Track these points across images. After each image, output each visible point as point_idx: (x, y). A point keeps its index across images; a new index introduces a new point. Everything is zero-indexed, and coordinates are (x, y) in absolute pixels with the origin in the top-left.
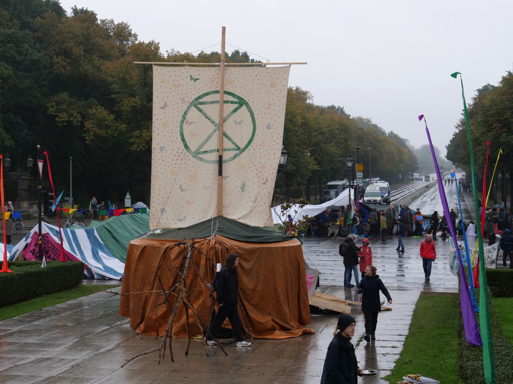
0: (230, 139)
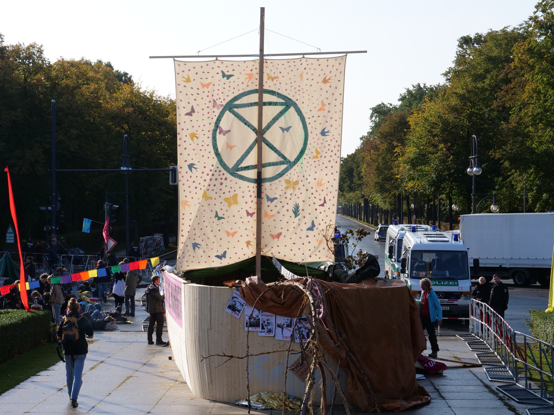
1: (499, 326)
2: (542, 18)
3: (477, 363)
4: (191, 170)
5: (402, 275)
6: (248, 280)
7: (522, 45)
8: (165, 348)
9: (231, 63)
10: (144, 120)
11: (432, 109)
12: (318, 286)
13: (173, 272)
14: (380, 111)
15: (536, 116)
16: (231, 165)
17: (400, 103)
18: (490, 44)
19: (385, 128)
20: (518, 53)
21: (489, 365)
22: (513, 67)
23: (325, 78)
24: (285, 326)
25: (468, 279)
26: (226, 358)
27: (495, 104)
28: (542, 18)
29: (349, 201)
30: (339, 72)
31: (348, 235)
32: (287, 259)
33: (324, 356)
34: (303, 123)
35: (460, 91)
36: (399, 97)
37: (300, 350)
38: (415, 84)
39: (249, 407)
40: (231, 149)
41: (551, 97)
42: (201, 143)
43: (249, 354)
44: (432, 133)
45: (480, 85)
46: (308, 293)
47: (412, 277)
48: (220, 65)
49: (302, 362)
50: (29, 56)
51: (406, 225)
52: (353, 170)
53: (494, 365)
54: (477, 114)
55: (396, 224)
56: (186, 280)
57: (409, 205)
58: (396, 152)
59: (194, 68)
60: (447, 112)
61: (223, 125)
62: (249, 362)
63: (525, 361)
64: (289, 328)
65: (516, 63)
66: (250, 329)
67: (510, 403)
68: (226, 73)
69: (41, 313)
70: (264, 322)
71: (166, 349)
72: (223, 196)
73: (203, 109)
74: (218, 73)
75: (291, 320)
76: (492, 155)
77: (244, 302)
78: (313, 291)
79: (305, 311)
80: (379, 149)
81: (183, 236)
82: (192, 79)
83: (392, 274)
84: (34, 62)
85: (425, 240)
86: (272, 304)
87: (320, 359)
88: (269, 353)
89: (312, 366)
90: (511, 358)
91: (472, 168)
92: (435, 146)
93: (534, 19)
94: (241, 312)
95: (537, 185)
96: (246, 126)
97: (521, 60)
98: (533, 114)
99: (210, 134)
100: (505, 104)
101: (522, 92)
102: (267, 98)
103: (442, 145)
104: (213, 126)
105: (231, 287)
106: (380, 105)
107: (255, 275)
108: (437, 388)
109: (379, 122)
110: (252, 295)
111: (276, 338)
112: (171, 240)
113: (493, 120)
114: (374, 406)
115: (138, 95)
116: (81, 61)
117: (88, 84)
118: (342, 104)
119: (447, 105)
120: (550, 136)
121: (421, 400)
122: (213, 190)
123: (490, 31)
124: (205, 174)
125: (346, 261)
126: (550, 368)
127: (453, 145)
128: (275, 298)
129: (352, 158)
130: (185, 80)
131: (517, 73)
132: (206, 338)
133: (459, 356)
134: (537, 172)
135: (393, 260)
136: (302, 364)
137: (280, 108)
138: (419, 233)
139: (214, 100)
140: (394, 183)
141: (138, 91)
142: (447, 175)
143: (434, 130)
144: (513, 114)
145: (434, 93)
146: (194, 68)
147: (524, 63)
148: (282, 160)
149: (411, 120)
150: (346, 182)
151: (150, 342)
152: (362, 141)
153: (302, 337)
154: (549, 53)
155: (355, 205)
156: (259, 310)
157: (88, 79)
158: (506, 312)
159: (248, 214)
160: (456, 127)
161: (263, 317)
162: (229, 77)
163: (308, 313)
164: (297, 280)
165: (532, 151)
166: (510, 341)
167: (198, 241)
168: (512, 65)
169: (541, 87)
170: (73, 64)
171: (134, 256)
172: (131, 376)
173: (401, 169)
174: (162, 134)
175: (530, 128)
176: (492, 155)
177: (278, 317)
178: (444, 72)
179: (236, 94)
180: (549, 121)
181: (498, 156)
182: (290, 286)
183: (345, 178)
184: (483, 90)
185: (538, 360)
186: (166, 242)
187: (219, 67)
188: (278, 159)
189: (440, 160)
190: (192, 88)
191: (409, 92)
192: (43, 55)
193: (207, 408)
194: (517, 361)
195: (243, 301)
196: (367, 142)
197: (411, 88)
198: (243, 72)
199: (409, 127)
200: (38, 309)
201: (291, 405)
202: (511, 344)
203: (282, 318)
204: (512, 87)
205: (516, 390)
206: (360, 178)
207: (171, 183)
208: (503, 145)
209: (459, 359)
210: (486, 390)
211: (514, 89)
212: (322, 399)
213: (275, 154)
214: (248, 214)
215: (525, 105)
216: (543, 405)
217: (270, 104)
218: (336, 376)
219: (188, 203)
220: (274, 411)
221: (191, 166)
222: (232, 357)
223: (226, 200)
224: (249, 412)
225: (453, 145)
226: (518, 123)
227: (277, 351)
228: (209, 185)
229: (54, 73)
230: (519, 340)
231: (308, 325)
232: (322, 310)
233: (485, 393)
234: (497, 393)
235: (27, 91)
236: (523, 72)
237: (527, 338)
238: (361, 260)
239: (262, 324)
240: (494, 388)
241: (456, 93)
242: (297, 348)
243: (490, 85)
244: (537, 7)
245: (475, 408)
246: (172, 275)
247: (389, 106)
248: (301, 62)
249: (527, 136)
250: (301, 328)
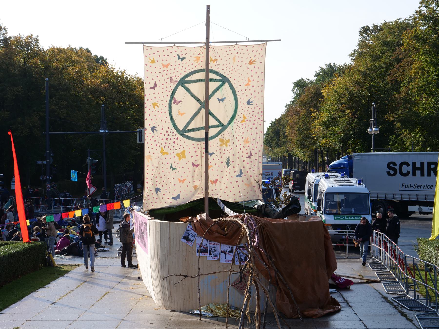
1: (394, 252)
2: (425, 12)
3: (377, 280)
4: (153, 132)
5: (318, 212)
6: (198, 217)
7: (410, 33)
8: (135, 270)
9: (185, 48)
10: (117, 93)
11: (340, 83)
12: (253, 221)
13: (140, 211)
14: (300, 85)
15: (421, 88)
16: (181, 128)
17: (316, 78)
18: (386, 31)
19: (304, 98)
20: (407, 38)
21: (386, 281)
22: (403, 50)
23: (251, 60)
24: (227, 252)
25: (369, 214)
26: (182, 278)
27: (389, 79)
28: (425, 12)
29: (277, 154)
30: (261, 56)
31: (276, 181)
32: (230, 200)
33: (258, 275)
34: (234, 96)
35: (363, 69)
36: (315, 74)
37: (239, 271)
38: (328, 63)
39: (200, 315)
41: (432, 73)
42: (160, 111)
43: (200, 274)
44: (340, 101)
45: (377, 64)
46: (245, 226)
47: (326, 213)
48: (176, 49)
49: (241, 280)
50: (28, 45)
51: (321, 173)
52: (280, 131)
53: (390, 281)
54: (375, 86)
55: (313, 172)
56: (151, 217)
57: (323, 157)
58: (313, 116)
59: (158, 52)
60: (352, 85)
61: (177, 96)
62: (200, 280)
63: (414, 277)
64: (230, 254)
65: (405, 47)
66: (201, 254)
67: (402, 310)
68: (181, 56)
69: (39, 243)
70: (211, 249)
71: (135, 271)
72: (176, 152)
73: (163, 84)
74: (175, 56)
75: (232, 248)
76: (387, 118)
77: (196, 233)
78: (249, 225)
79: (243, 241)
80: (299, 114)
81: (147, 183)
82: (156, 61)
83: (311, 211)
84: (31, 50)
85: (336, 185)
86: (217, 235)
87: (255, 278)
88: (215, 273)
89: (249, 283)
90: (403, 275)
91: (371, 128)
92: (343, 112)
93: (419, 12)
94: (193, 241)
95: (422, 141)
96: (192, 98)
97: (409, 44)
98: (419, 86)
99: (167, 104)
100: (397, 79)
101: (410, 69)
102: (212, 76)
103: (348, 111)
104: (169, 98)
105: (185, 222)
106: (300, 80)
107: (204, 213)
108: (346, 299)
109: (299, 93)
110: (202, 228)
111: (221, 262)
112: (139, 186)
113: (388, 90)
114: (297, 314)
115: (111, 73)
116: (68, 48)
117: (73, 66)
118: (263, 80)
119: (352, 80)
120: (432, 103)
121: (334, 308)
122: (168, 147)
123: (384, 22)
124: (163, 134)
125: (274, 201)
126: (433, 283)
127: (356, 111)
128: (219, 230)
129: (279, 121)
130: (151, 61)
131: (406, 55)
132: (167, 262)
133: (363, 275)
134: (422, 131)
135: (311, 200)
136: (241, 281)
137: (219, 83)
138: (331, 179)
139: (171, 77)
140: (311, 141)
141: (112, 71)
142: (353, 134)
143: (342, 99)
144: (403, 86)
145: (342, 70)
146: (158, 52)
147: (411, 47)
149: (324, 92)
150: (274, 140)
151: (123, 265)
152: (286, 108)
153: (241, 261)
154: (431, 39)
155: (281, 158)
156: (207, 240)
157: (73, 62)
158: (399, 240)
160: (359, 97)
161: (210, 245)
162: (182, 59)
163: (245, 242)
164: (237, 217)
165: (418, 115)
166: (402, 263)
167: (159, 186)
168: (402, 48)
169: (425, 65)
170: (61, 50)
171: (109, 198)
172: (109, 292)
173: (317, 129)
174: (131, 104)
175: (417, 97)
176: (387, 118)
177: (222, 245)
178: (350, 53)
179: (187, 72)
180: (431, 92)
181: (392, 119)
182: (231, 221)
183: (274, 137)
184: (380, 68)
185: (424, 277)
186: (135, 188)
187: (175, 51)
188: (216, 123)
189: (346, 122)
190: (156, 68)
191: (323, 70)
192: (38, 44)
193: (168, 316)
194: (407, 278)
195: (195, 233)
196: (291, 110)
197: (324, 67)
198: (193, 56)
199: (322, 97)
200: (36, 240)
201: (233, 313)
202: (403, 264)
203: (225, 246)
204: (402, 65)
205: (407, 300)
206: (285, 137)
207: (138, 142)
208: (396, 110)
209: (363, 276)
210: (384, 300)
211: (404, 67)
212: (257, 308)
213: (213, 119)
215: (412, 79)
216: (428, 312)
217: (211, 80)
218: (267, 290)
219: (151, 157)
220: (220, 318)
221: (153, 129)
222: (186, 276)
223: (177, 155)
224: (200, 319)
225: (356, 111)
226: (407, 93)
227: (221, 272)
228: (166, 143)
229: (47, 58)
230: (409, 262)
231: (245, 251)
232: (256, 239)
233: (383, 303)
234: (393, 303)
235: (26, 72)
236: (410, 54)
237: (415, 260)
238: (286, 201)
239: (210, 251)
240: (390, 299)
241: (359, 71)
242: (237, 269)
243: (385, 63)
244: (421, 3)
245: (376, 315)
246: (140, 213)
247: (307, 80)
248: (234, 48)
249: (414, 103)
250: (240, 253)
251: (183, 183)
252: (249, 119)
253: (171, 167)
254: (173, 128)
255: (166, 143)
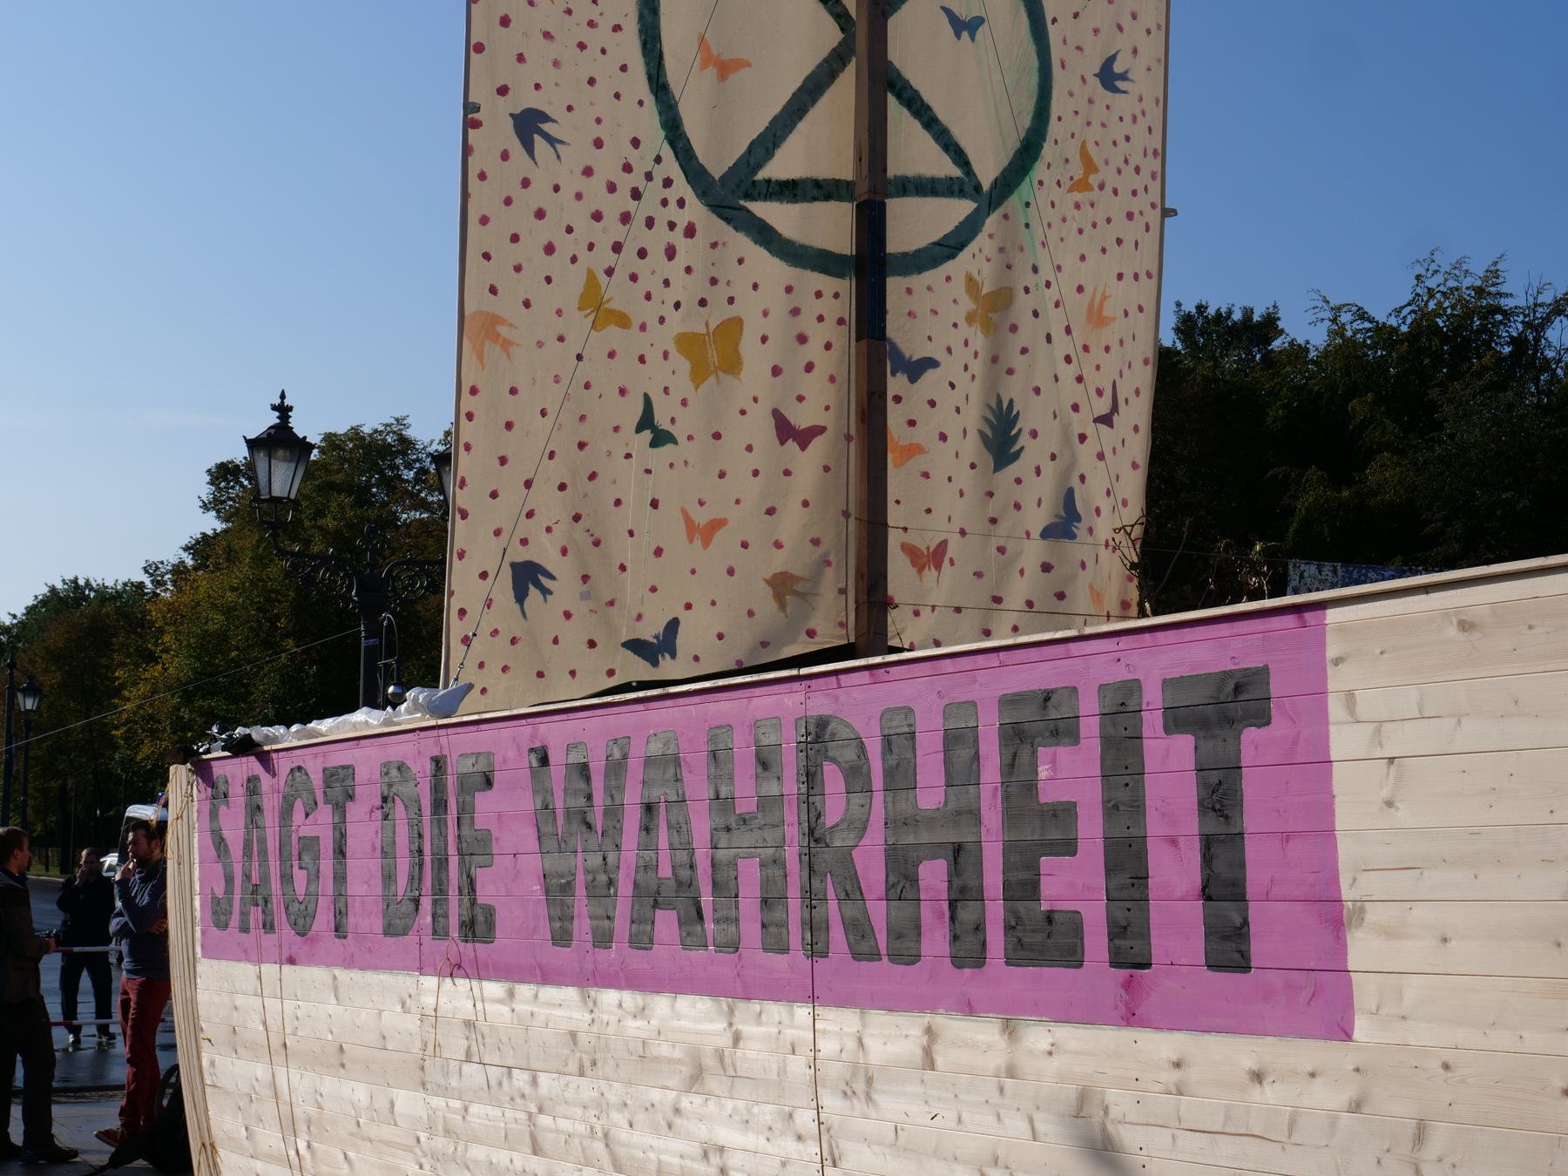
0: (930, 122)
16: (718, 159)
40: (722, 76)
148: (956, 172)
159: (785, 430)
214: (785, 430)
251: (706, 544)
252: (1112, 180)
253: (646, 421)
254: (667, 153)
255: (617, 248)
